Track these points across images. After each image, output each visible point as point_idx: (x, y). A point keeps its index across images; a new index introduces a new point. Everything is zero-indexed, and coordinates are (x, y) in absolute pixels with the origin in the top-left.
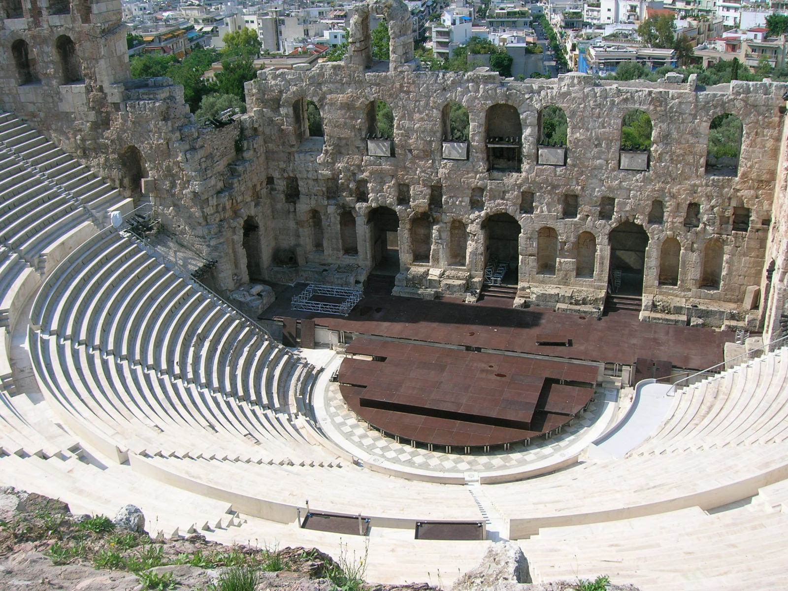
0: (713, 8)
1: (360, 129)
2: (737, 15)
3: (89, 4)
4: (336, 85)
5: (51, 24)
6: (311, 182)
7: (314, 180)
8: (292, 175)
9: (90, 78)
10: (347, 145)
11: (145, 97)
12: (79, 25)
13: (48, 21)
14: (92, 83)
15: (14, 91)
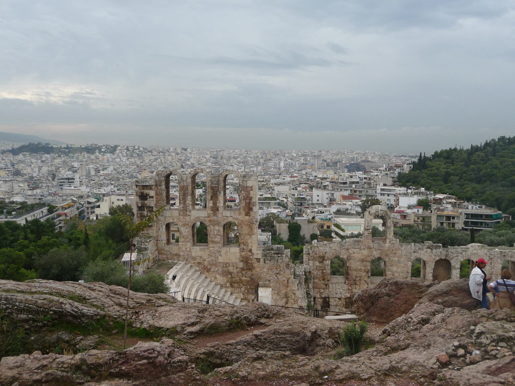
0: (375, 194)
1: (367, 272)
2: (388, 198)
3: (251, 206)
4: (358, 250)
5: (224, 215)
6: (337, 300)
7: (340, 299)
8: (327, 296)
9: (244, 244)
10: (360, 280)
11: (276, 255)
12: (243, 217)
13: (222, 213)
14: (245, 248)
15: (188, 250)
